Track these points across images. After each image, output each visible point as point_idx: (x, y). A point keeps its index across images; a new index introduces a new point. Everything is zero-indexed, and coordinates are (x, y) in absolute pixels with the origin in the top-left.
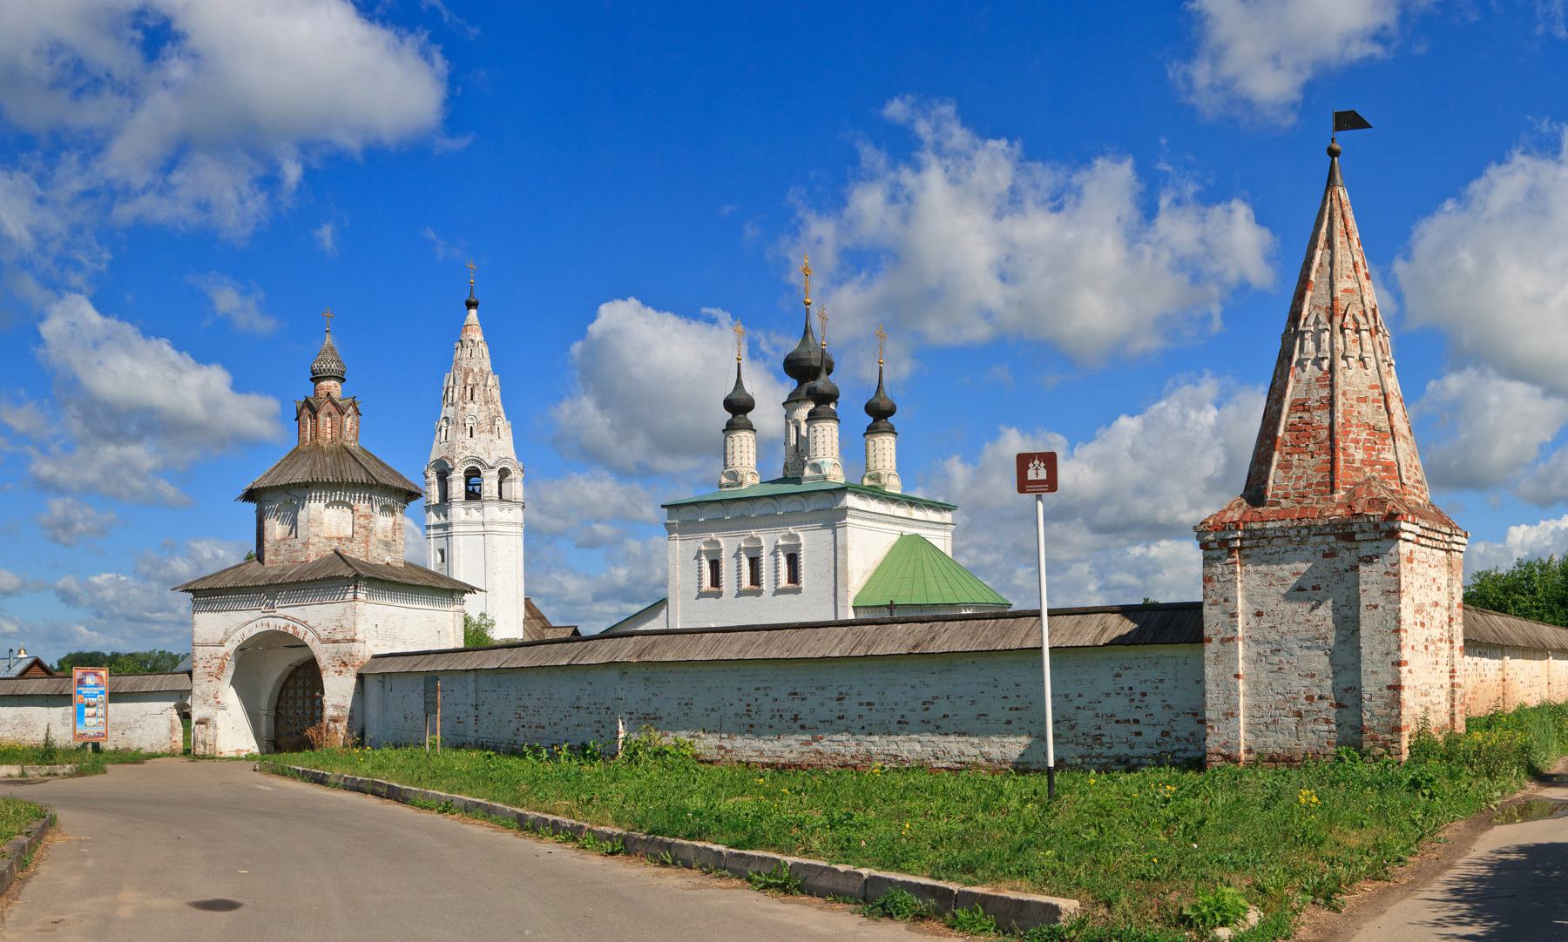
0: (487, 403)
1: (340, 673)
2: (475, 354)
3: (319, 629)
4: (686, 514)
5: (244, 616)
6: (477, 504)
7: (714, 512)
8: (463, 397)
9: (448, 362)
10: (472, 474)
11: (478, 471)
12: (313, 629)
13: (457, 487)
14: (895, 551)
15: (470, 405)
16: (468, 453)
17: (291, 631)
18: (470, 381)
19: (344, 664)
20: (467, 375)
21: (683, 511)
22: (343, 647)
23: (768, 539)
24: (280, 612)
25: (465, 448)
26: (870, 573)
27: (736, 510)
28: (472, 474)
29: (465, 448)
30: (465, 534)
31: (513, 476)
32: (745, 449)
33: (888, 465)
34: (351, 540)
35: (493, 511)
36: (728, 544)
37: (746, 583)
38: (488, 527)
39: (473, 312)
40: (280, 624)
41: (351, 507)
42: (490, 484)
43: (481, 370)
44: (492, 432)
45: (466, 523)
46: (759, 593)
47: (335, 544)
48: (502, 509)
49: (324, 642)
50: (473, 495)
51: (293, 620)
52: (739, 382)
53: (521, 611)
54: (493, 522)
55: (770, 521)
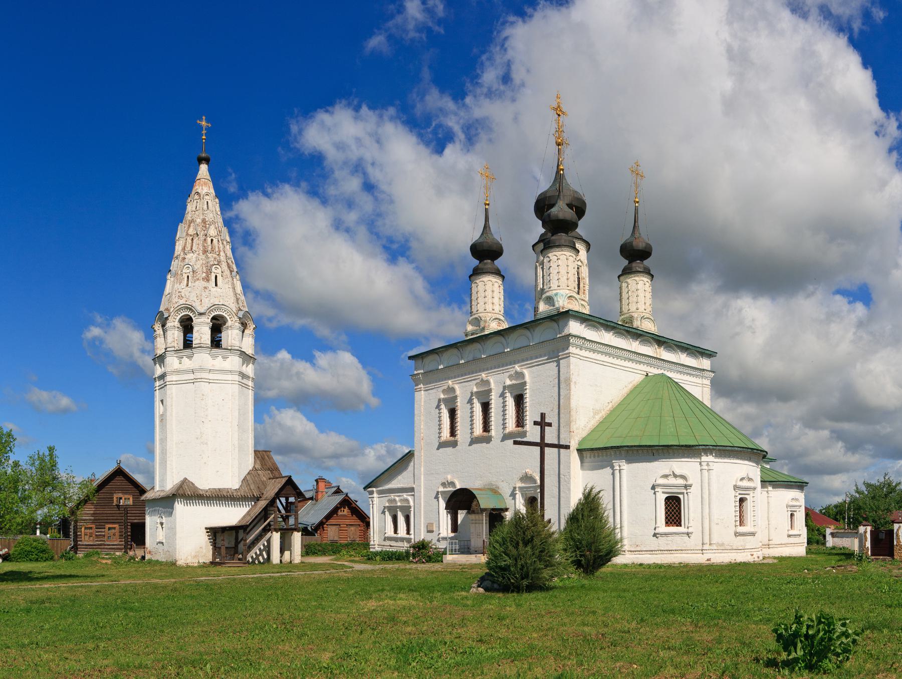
0: (205, 252)
4: (430, 363)
6: (188, 351)
7: (450, 358)
8: (184, 249)
10: (187, 326)
11: (190, 319)
13: (175, 336)
14: (636, 391)
16: (181, 302)
21: (427, 360)
23: (497, 381)
25: (180, 297)
26: (603, 414)
27: (471, 352)
28: (187, 326)
29: (180, 297)
30: (178, 383)
31: (229, 323)
32: (489, 293)
33: (642, 307)
35: (203, 358)
36: (463, 389)
37: (478, 430)
38: (198, 375)
42: (202, 333)
43: (204, 221)
44: (207, 279)
45: (178, 372)
46: (488, 440)
48: (214, 357)
50: (187, 344)
52: (486, 227)
53: (249, 462)
54: (202, 370)
55: (499, 361)
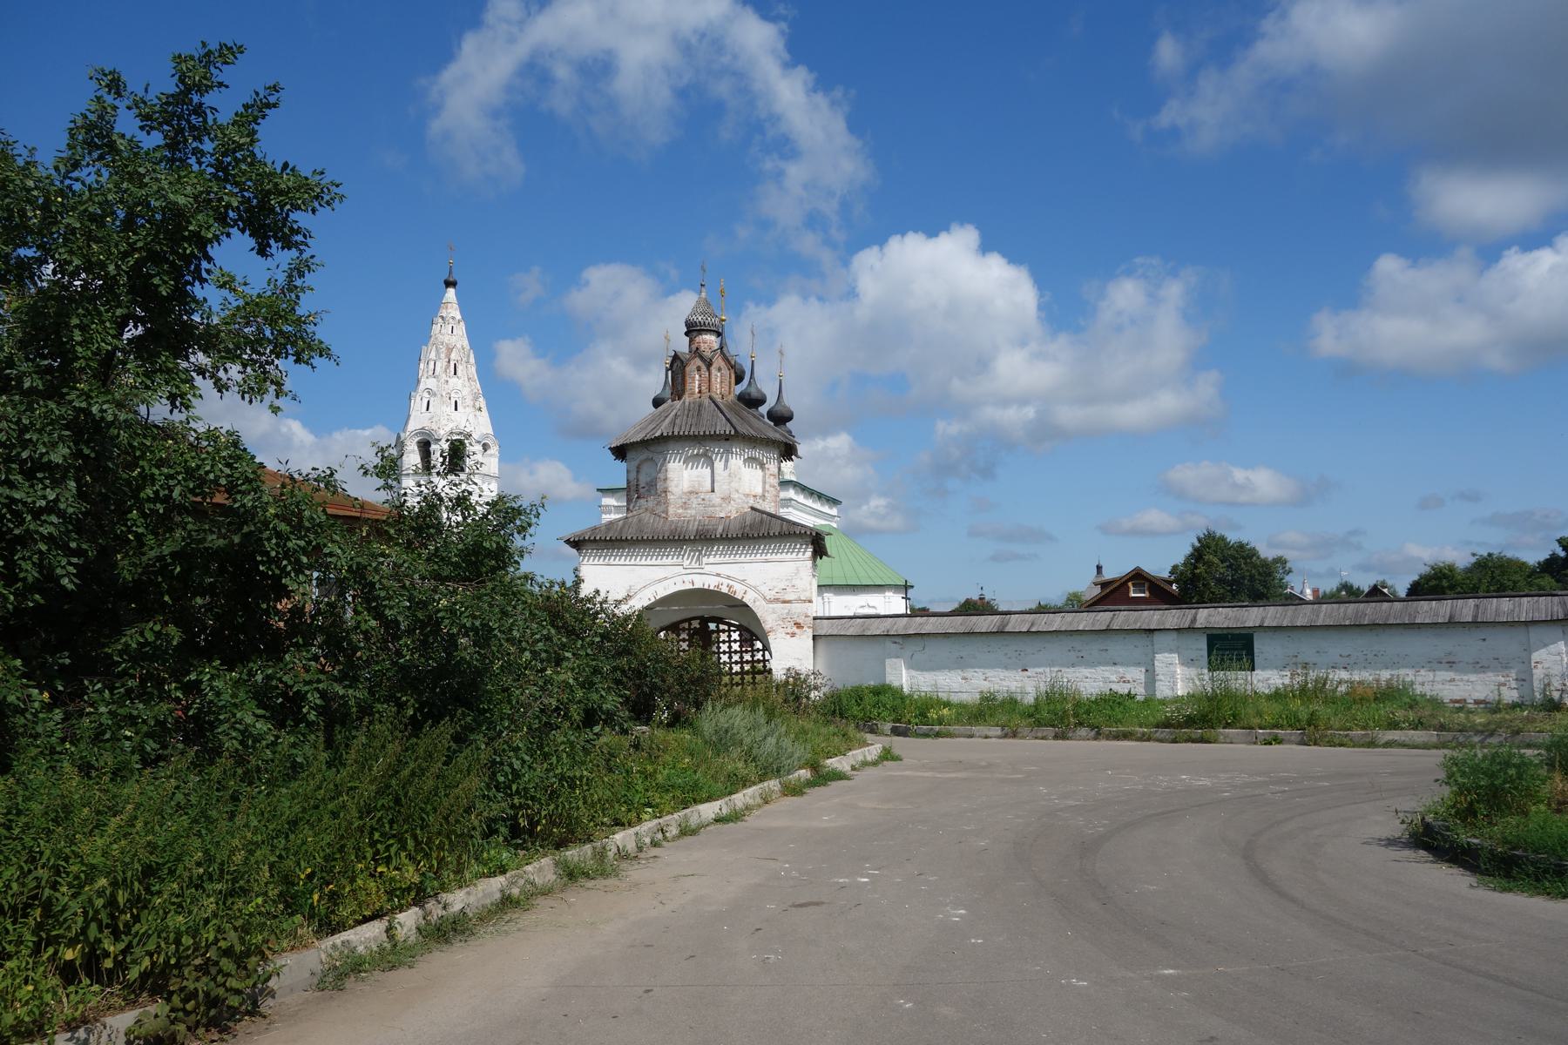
1: (793, 635)
2: (451, 329)
3: (764, 589)
5: (660, 573)
9: (426, 337)
12: (755, 589)
15: (454, 380)
17: (725, 590)
18: (453, 356)
19: (798, 625)
20: (450, 350)
22: (797, 608)
24: (708, 569)
34: (763, 497)
39: (451, 292)
40: (709, 583)
41: (762, 466)
47: (751, 502)
49: (770, 601)
51: (728, 577)
